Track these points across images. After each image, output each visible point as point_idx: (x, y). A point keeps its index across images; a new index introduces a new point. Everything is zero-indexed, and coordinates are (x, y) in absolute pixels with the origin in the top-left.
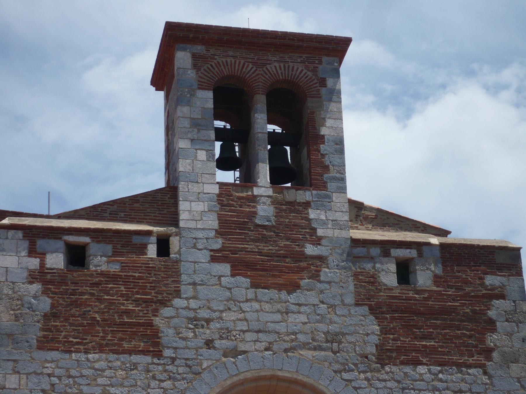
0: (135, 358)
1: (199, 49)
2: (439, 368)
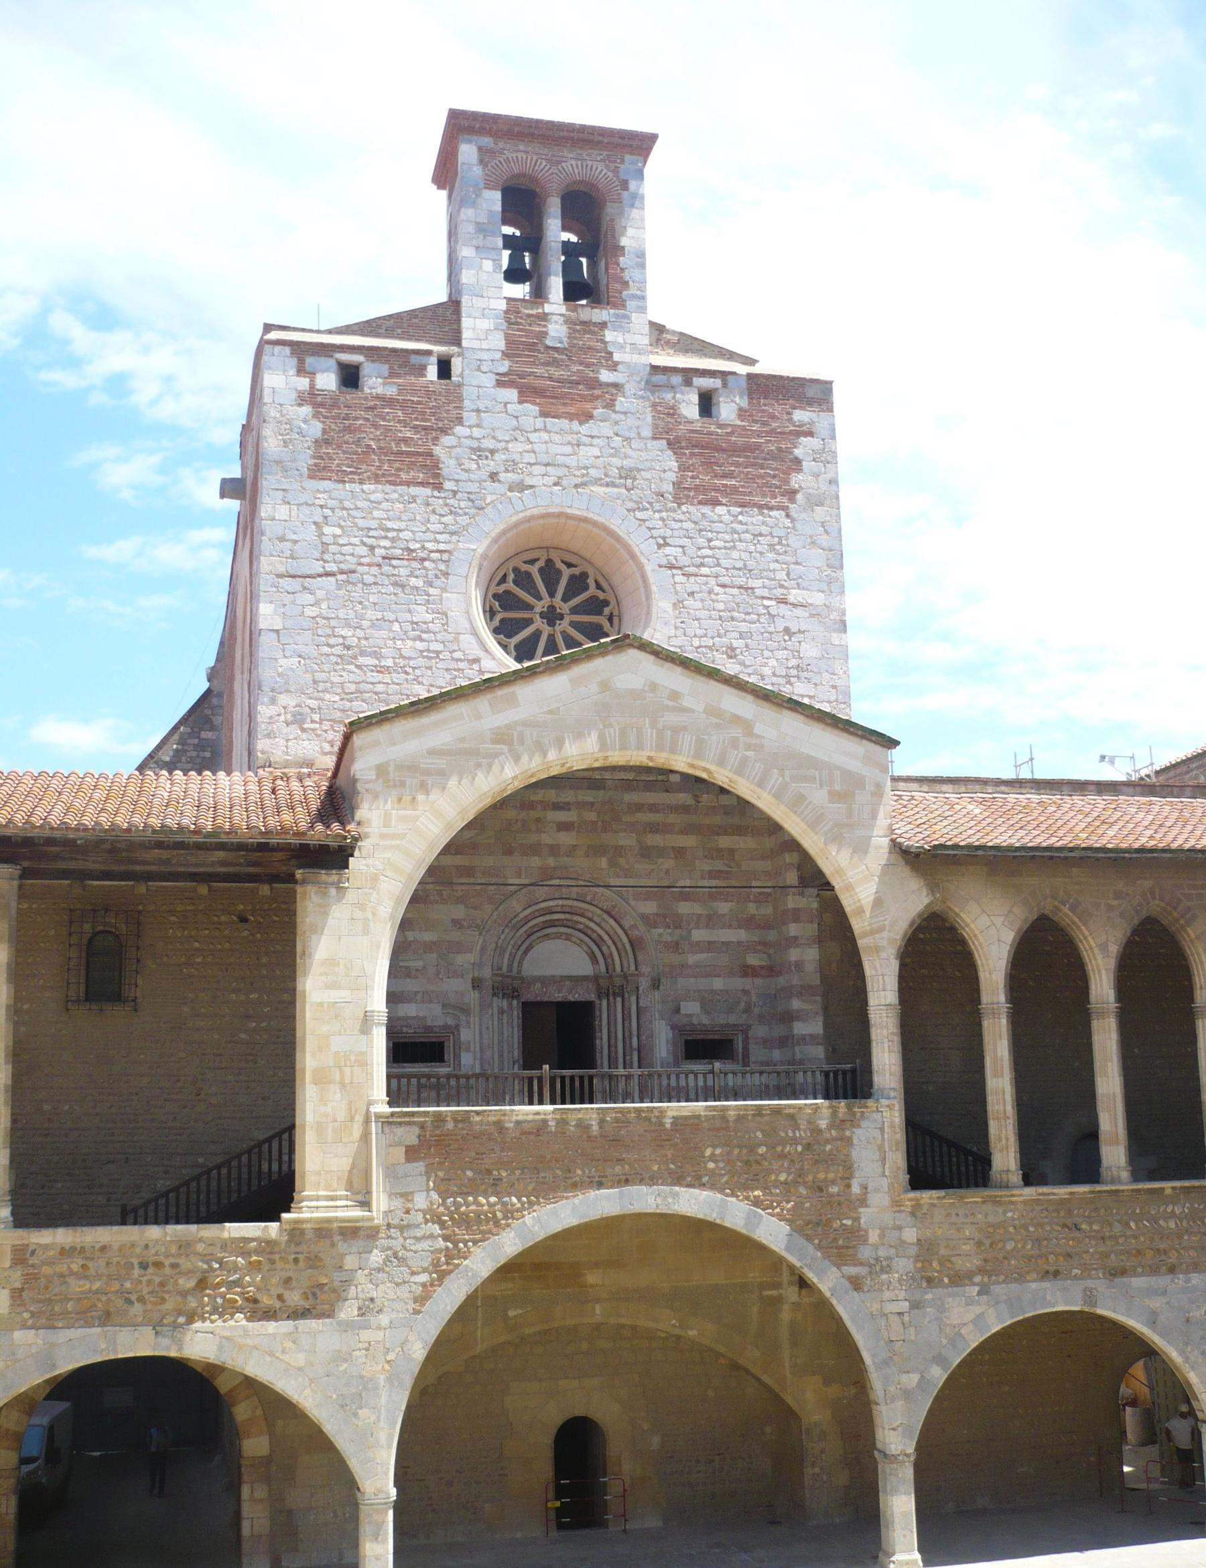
0: (414, 490)
1: (487, 141)
2: (739, 510)
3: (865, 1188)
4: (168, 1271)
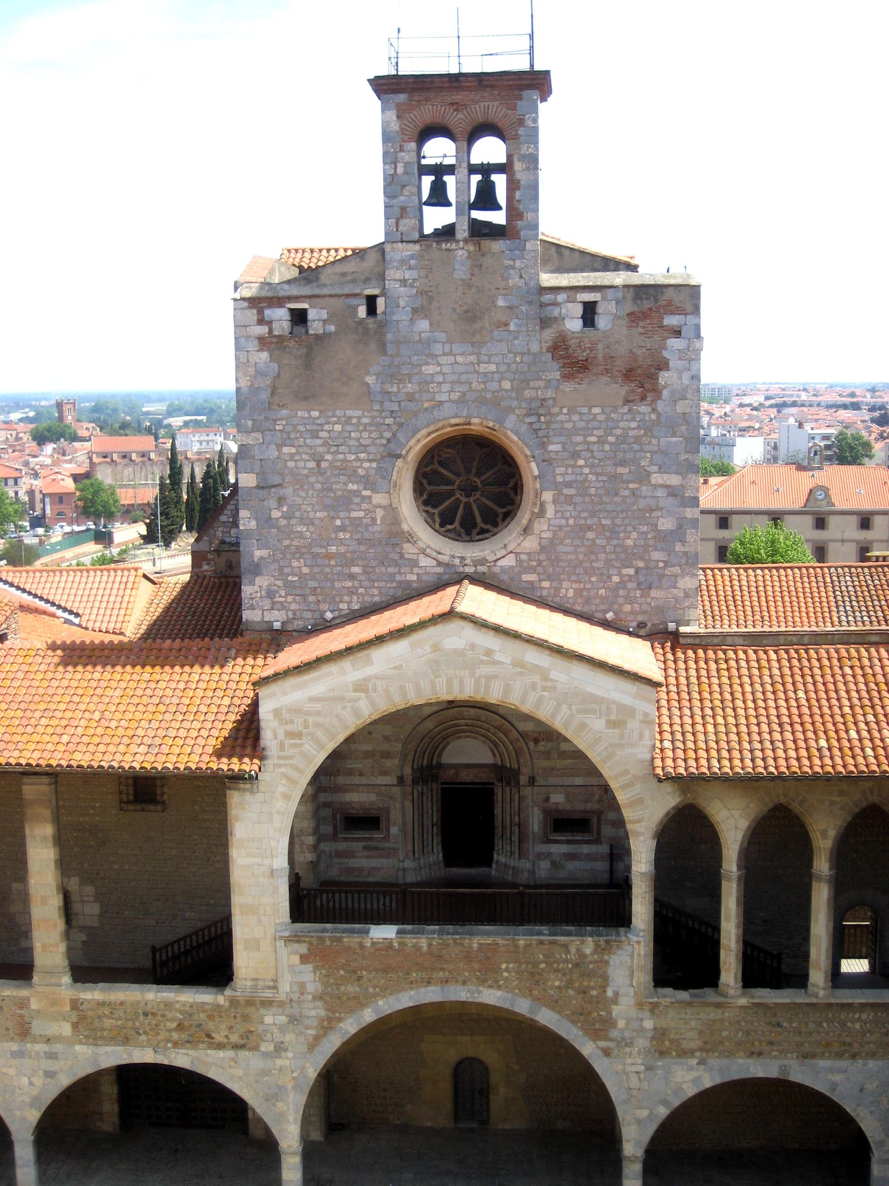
3: (616, 994)
4: (159, 1018)
